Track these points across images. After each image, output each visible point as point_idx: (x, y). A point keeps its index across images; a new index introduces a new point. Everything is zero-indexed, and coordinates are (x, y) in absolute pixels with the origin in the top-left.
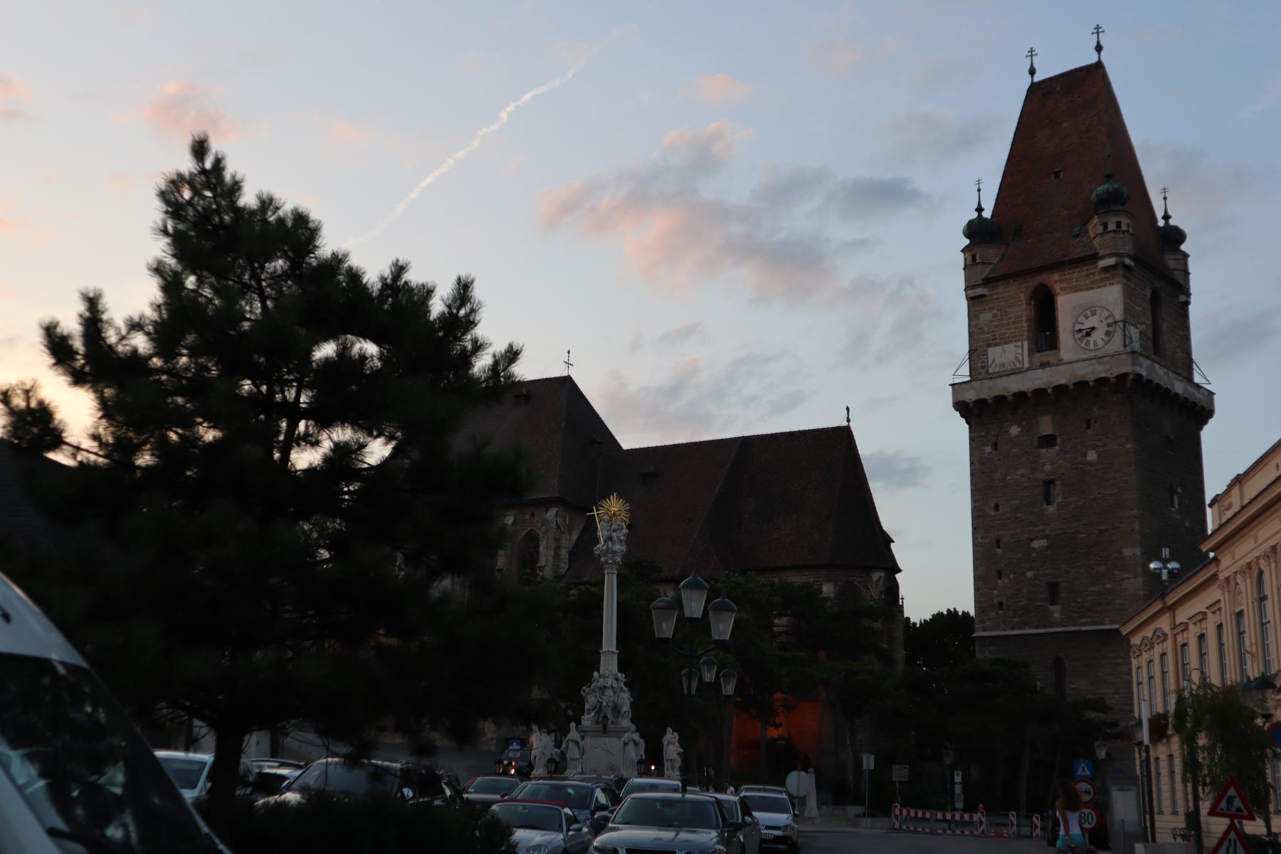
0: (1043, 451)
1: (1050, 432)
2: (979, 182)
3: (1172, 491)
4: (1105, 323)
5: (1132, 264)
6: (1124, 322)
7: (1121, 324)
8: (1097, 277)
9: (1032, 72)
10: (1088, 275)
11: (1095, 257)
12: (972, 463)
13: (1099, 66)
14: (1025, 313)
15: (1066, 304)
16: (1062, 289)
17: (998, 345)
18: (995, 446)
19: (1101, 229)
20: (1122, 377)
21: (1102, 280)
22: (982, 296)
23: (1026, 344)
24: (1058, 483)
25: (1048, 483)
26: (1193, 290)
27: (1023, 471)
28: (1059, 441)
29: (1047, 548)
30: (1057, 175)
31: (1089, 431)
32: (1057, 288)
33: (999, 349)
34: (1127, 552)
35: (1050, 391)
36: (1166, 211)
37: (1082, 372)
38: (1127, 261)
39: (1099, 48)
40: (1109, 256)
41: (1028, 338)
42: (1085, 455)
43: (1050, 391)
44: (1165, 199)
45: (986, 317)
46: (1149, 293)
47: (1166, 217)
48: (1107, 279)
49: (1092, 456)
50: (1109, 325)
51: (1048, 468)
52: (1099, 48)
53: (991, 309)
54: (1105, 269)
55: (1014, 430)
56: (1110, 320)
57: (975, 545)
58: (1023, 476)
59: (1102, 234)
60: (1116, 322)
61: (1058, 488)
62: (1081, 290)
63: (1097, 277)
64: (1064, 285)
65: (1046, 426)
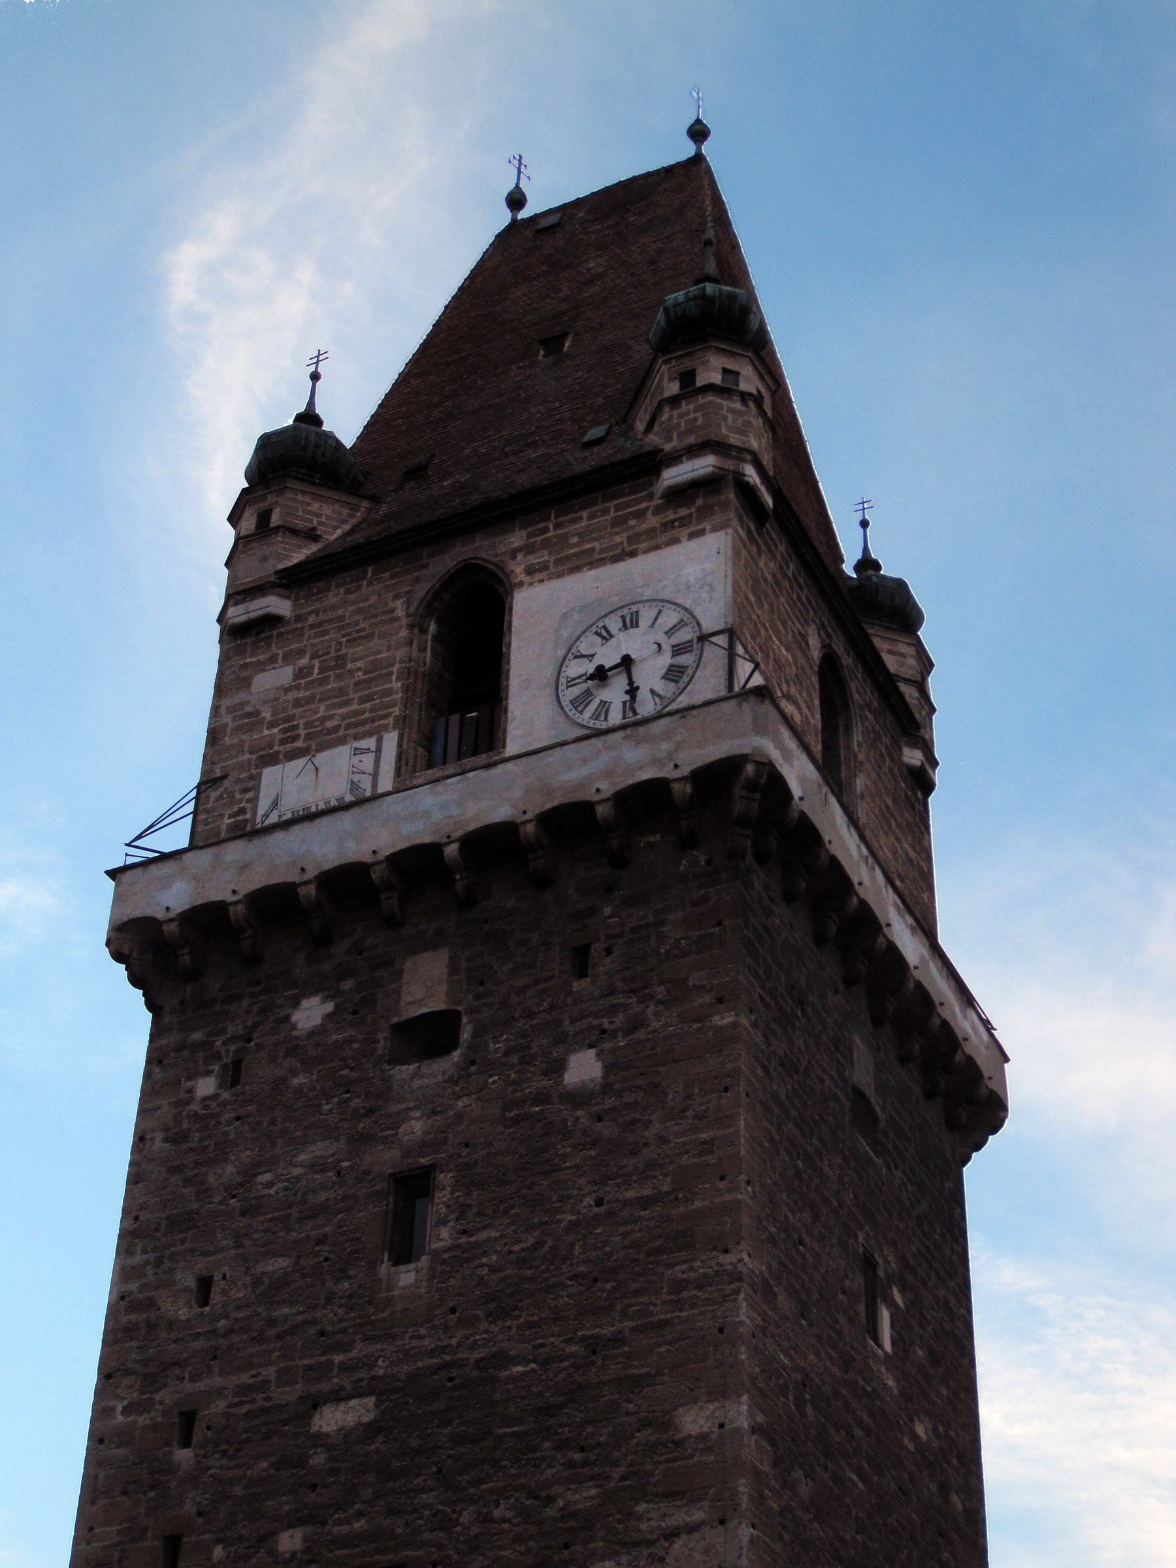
0: (403, 1072)
1: (438, 1003)
2: (318, 358)
3: (875, 1293)
4: (666, 660)
5: (770, 502)
6: (731, 633)
7: (722, 640)
8: (652, 521)
9: (516, 200)
10: (616, 522)
11: (651, 463)
12: (141, 1139)
13: (698, 159)
14: (400, 654)
15: (546, 616)
16: (530, 571)
17: (292, 756)
18: (233, 1075)
19: (673, 388)
20: (717, 777)
21: (667, 526)
22: (271, 620)
23: (391, 741)
24: (445, 1178)
25: (413, 1186)
26: (946, 732)
27: (320, 1149)
28: (466, 1035)
29: (372, 1430)
30: (553, 344)
31: (576, 986)
32: (517, 568)
33: (298, 763)
34: (694, 1421)
35: (451, 850)
36: (866, 550)
37: (572, 776)
38: (751, 473)
39: (698, 133)
40: (693, 451)
41: (402, 723)
42: (558, 1067)
43: (451, 850)
44: (864, 524)
45: (273, 679)
46: (814, 642)
47: (867, 564)
48: (684, 522)
49: (584, 1068)
50: (678, 650)
51: (416, 1128)
52: (698, 133)
53: (288, 658)
54: (680, 494)
55: (311, 1013)
56: (685, 635)
57: (97, 1439)
58: (317, 1166)
59: (674, 401)
60: (703, 638)
61: (442, 1197)
62: (601, 562)
63: (652, 521)
64: (544, 556)
65: (425, 984)
